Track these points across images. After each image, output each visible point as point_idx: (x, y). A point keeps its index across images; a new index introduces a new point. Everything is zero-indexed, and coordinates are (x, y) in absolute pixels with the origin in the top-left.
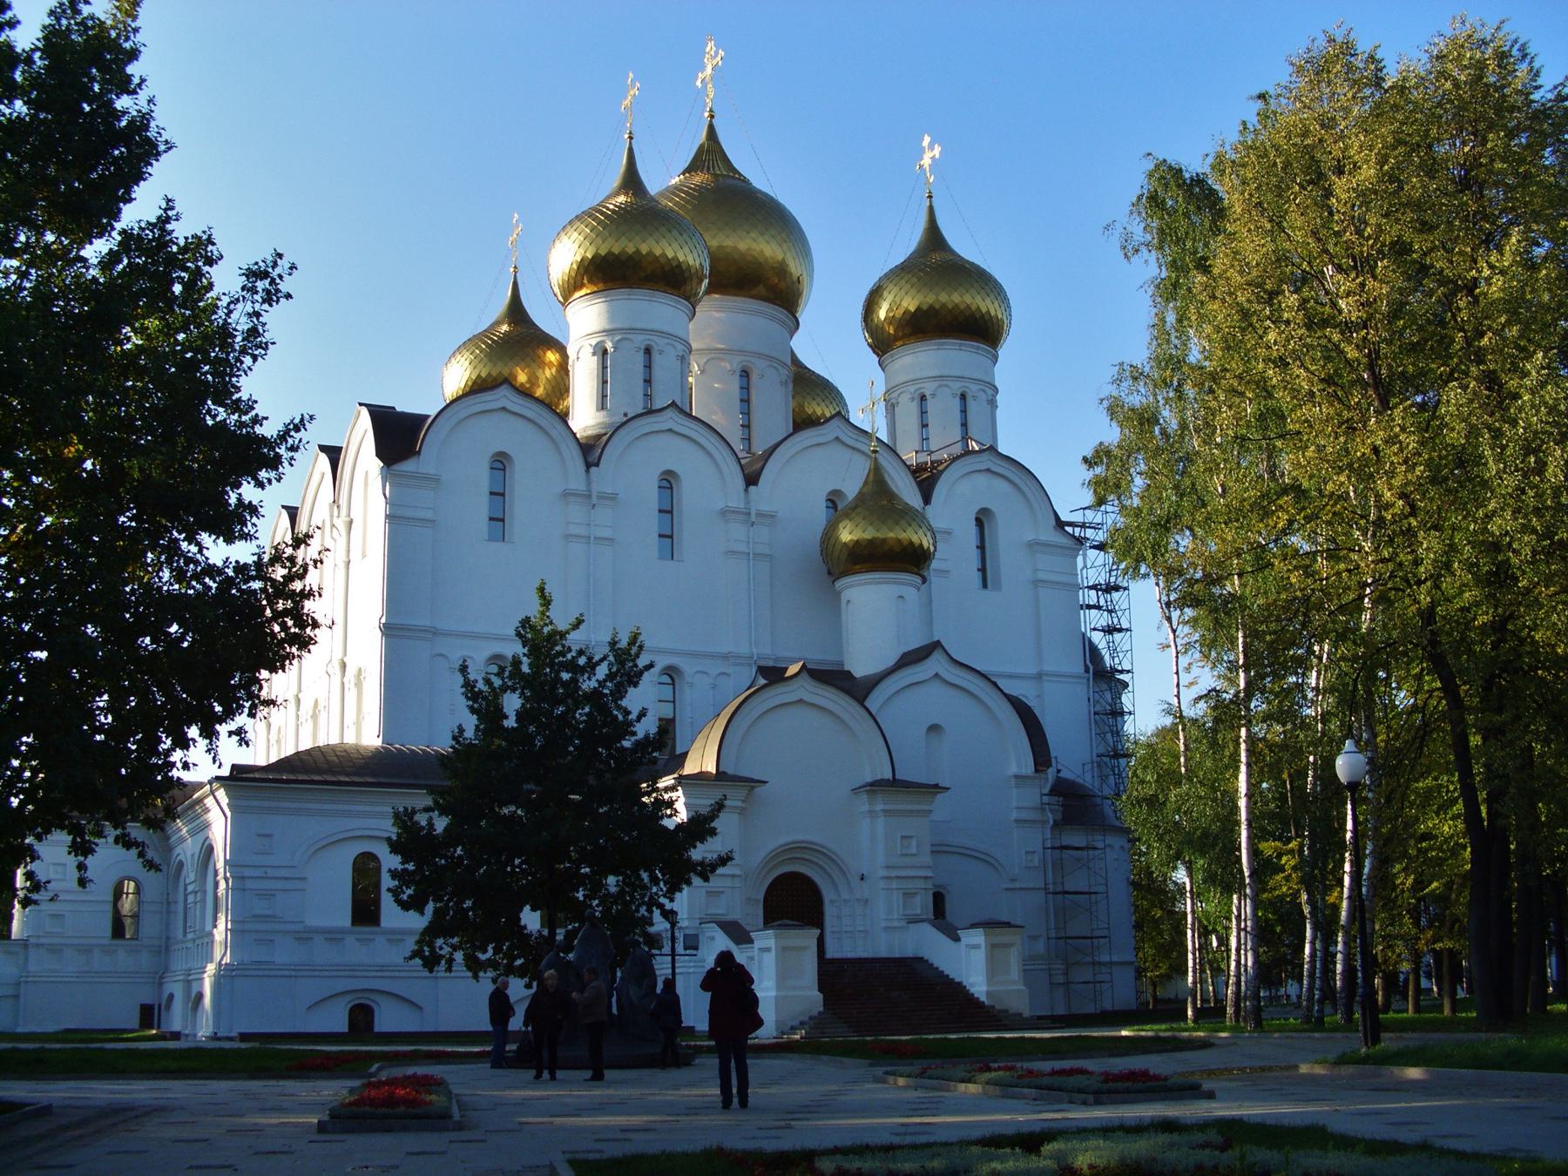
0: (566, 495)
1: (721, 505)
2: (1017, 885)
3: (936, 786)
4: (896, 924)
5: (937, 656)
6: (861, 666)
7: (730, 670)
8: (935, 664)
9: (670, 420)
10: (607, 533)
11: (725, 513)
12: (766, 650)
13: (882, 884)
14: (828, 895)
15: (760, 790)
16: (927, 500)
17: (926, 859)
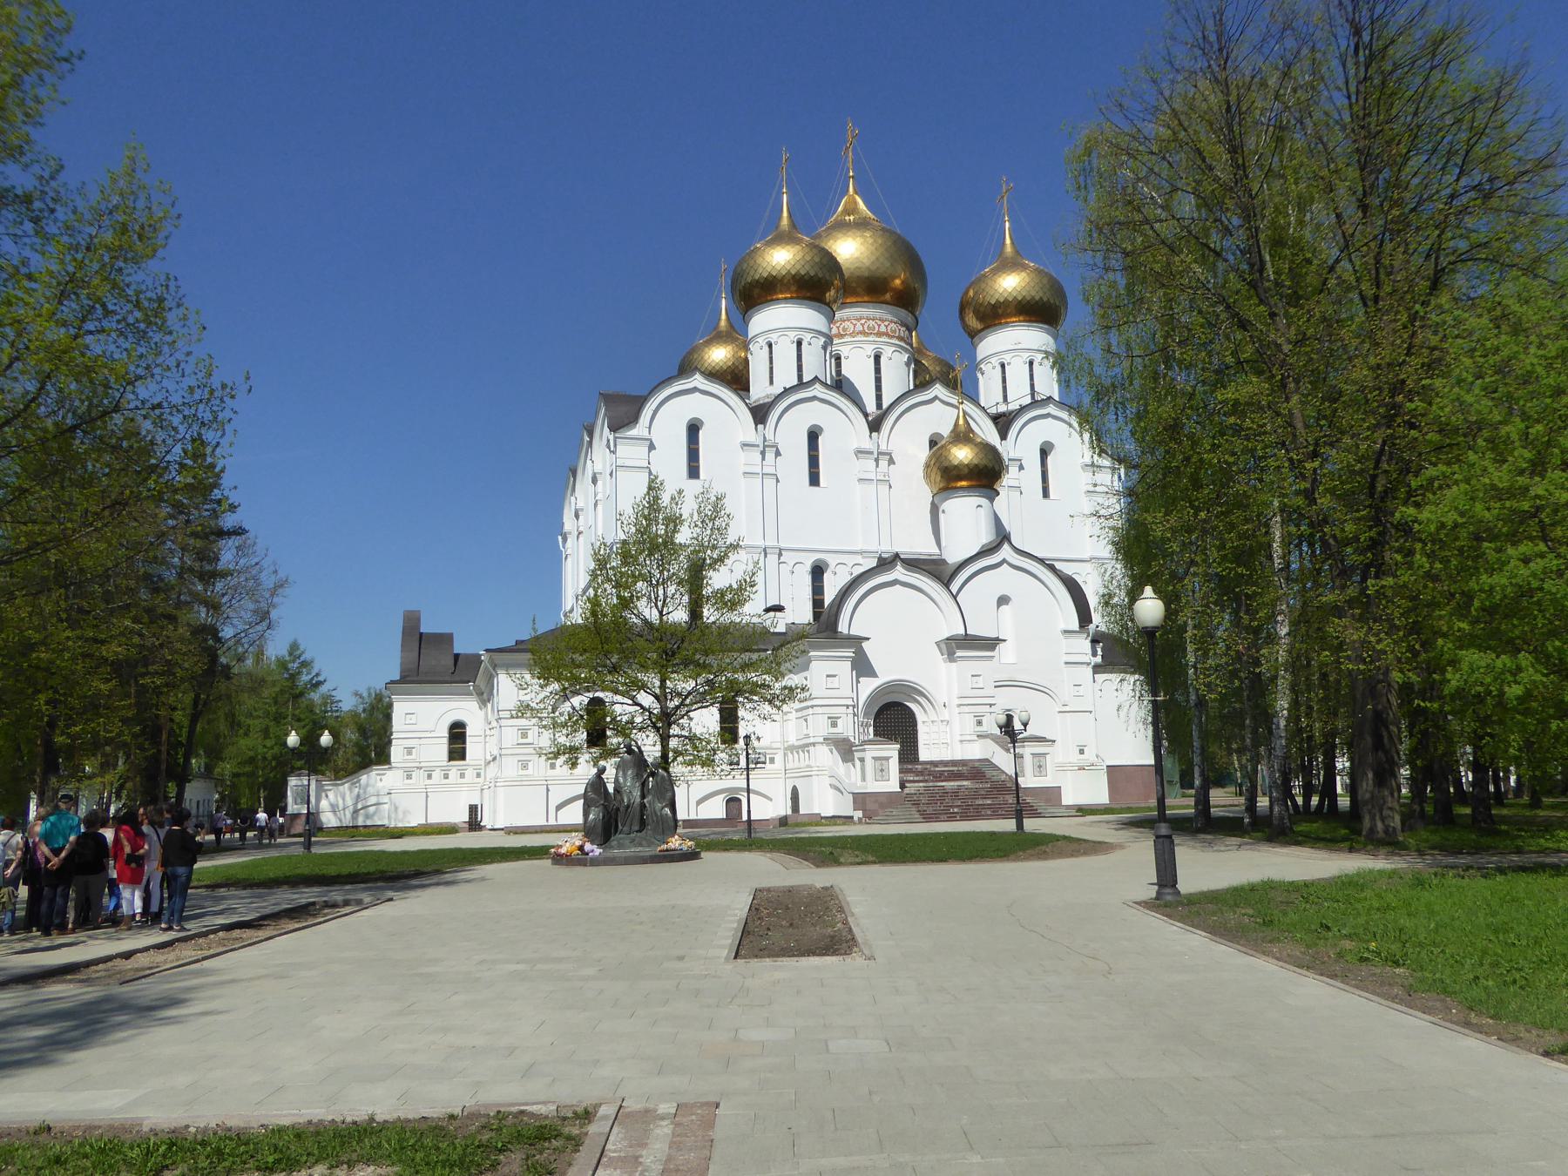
0: (745, 445)
1: (855, 446)
2: (1067, 709)
3: (997, 639)
4: (968, 738)
5: (1006, 546)
6: (953, 556)
7: (861, 561)
8: (1005, 552)
9: (818, 390)
10: (771, 470)
11: (860, 453)
12: (884, 548)
13: (957, 710)
14: (920, 716)
15: (865, 645)
16: (1003, 436)
17: (990, 691)
